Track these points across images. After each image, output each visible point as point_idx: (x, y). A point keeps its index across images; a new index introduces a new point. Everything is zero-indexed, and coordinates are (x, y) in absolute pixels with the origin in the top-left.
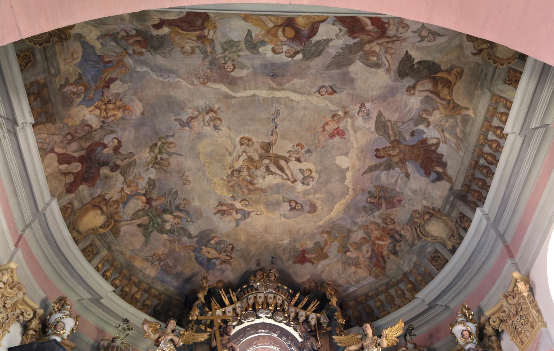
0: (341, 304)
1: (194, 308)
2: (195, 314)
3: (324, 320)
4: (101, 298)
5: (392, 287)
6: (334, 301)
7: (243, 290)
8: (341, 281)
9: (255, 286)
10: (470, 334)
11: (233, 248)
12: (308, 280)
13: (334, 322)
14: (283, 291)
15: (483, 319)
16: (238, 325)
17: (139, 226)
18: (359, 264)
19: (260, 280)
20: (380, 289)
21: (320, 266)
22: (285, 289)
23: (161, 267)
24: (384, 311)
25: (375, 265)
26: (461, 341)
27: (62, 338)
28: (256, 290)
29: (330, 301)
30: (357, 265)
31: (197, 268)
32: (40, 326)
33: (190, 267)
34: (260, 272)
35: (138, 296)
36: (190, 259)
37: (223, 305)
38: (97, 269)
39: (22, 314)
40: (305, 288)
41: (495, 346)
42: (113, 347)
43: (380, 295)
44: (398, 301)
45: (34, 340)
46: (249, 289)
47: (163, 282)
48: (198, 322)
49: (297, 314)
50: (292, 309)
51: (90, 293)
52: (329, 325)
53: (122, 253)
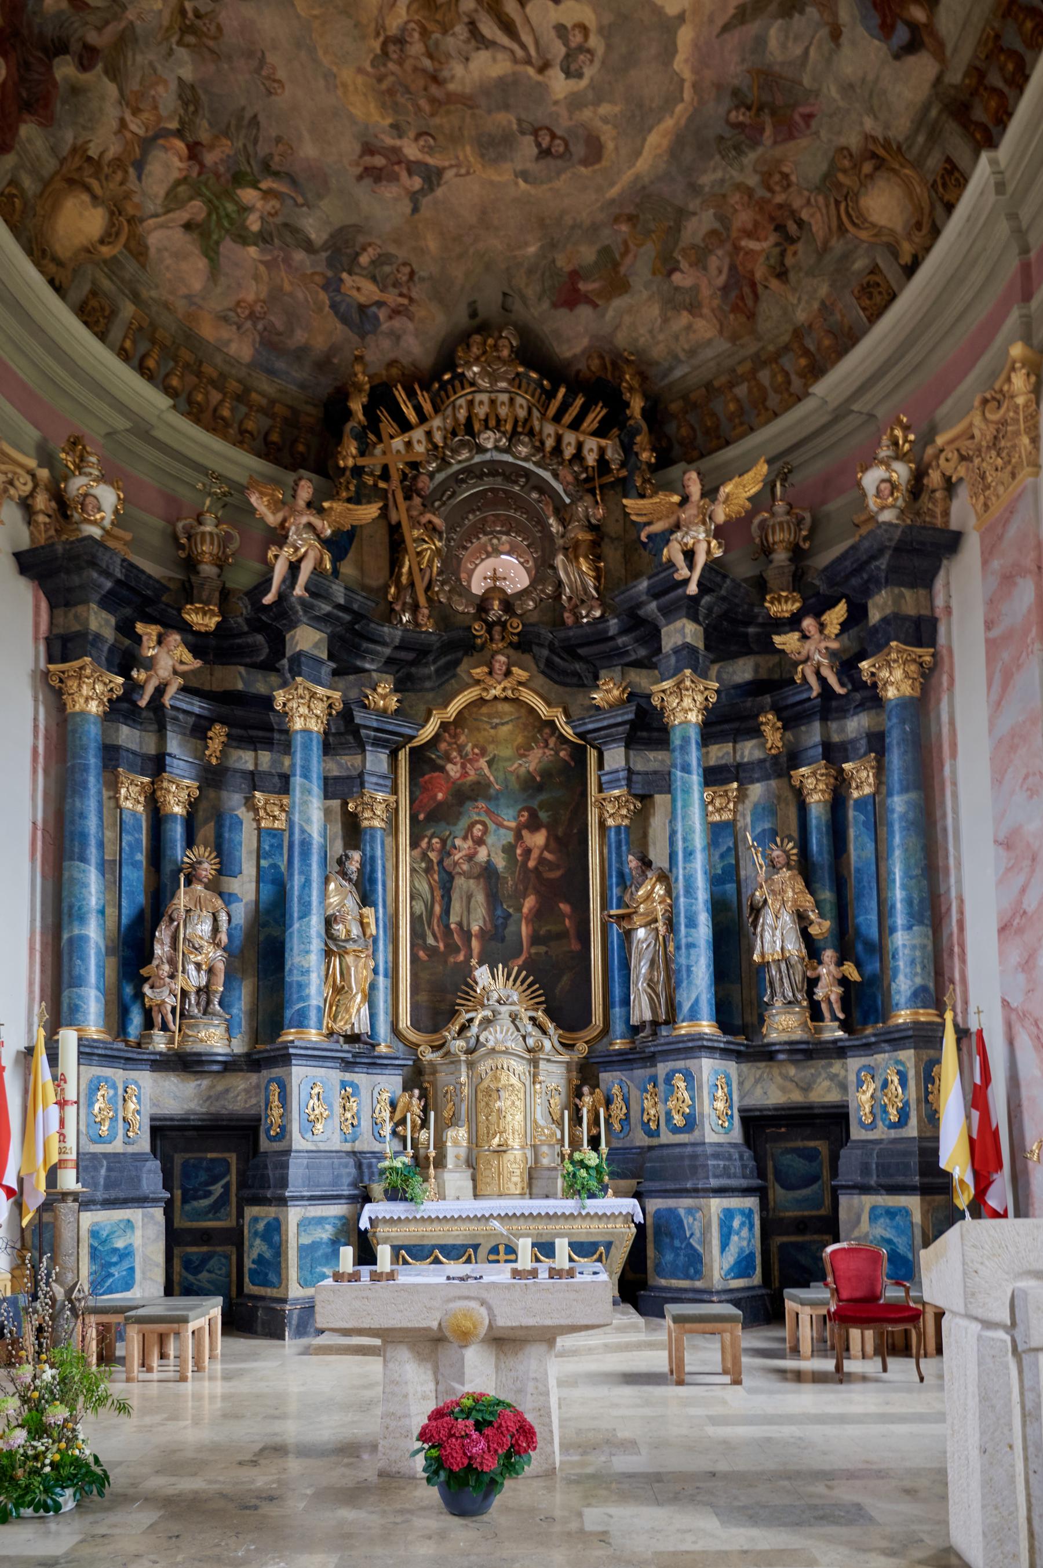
0: (654, 414)
1: (345, 439)
2: (349, 454)
3: (613, 454)
5: (764, 364)
6: (637, 404)
7: (443, 386)
8: (657, 352)
9: (469, 374)
11: (412, 274)
12: (583, 352)
13: (633, 459)
16: (439, 470)
17: (188, 226)
18: (700, 306)
19: (477, 360)
20: (740, 370)
21: (610, 313)
23: (260, 334)
24: (742, 424)
25: (735, 309)
27: (103, 529)
28: (472, 384)
29: (627, 405)
30: (693, 308)
31: (339, 330)
33: (322, 332)
34: (477, 338)
36: (320, 310)
37: (405, 426)
38: (124, 355)
40: (578, 372)
46: (457, 383)
47: (271, 372)
48: (358, 471)
50: (549, 429)
52: (623, 465)
53: (166, 306)
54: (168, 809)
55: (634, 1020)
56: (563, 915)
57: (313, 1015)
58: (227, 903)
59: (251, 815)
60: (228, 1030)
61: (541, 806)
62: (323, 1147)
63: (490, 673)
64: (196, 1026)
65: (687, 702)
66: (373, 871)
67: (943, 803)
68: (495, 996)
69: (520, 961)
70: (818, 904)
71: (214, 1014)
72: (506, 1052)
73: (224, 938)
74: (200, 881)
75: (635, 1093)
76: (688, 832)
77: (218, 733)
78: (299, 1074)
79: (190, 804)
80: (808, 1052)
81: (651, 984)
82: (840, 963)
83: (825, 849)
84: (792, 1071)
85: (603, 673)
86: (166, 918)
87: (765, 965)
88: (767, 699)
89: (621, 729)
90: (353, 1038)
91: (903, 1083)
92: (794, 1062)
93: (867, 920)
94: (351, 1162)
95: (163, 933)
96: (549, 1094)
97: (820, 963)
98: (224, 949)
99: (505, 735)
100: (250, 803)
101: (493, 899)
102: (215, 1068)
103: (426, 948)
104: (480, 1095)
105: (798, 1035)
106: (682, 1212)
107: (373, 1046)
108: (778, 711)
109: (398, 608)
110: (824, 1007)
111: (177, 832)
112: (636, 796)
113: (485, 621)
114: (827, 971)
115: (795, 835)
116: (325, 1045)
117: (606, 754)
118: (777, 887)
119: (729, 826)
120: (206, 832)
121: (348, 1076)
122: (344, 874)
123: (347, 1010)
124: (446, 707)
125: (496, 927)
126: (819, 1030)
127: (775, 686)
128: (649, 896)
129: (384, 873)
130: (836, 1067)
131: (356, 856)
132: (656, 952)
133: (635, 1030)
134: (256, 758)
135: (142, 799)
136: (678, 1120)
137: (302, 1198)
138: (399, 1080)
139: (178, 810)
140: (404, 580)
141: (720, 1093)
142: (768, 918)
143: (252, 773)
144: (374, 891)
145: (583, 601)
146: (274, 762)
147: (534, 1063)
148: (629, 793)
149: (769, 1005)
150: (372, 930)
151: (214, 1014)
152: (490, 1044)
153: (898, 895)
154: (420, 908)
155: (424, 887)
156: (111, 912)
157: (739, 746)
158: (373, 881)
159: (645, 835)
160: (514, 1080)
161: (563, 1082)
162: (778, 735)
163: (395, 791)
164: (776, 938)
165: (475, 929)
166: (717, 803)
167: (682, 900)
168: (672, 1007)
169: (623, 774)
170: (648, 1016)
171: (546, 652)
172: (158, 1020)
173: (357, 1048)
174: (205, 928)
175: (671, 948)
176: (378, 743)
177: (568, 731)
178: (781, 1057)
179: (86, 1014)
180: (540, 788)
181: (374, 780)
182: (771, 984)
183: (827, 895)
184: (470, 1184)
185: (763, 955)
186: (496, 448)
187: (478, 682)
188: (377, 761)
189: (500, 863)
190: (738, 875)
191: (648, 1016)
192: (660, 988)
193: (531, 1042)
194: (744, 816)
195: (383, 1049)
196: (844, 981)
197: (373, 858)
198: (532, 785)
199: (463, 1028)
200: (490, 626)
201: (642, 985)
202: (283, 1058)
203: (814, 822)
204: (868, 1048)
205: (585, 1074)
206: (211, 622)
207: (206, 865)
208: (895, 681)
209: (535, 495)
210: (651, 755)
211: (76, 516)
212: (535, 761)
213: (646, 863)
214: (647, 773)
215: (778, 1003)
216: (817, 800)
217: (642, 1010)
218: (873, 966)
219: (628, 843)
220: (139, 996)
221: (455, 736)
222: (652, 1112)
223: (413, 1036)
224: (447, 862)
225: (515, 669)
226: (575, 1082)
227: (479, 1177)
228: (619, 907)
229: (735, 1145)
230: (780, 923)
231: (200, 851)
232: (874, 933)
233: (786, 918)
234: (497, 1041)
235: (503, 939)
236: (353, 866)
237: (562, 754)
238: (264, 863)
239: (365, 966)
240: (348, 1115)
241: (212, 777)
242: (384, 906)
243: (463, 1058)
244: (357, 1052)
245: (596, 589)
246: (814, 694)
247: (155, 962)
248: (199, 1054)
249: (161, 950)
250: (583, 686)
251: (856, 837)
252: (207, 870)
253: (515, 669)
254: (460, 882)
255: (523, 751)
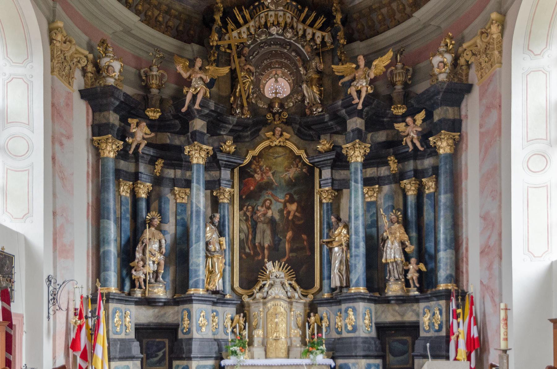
4: (132, 30)
10: (445, 65)
14: (292, 7)
15: (460, 49)
22: (294, 6)
26: (436, 71)
27: (115, 79)
32: (94, 69)
35: (161, 19)
39: (79, 62)
41: (464, 74)
42: (153, 75)
43: (383, 8)
44: (398, 16)
45: (93, 80)
49: (305, 31)
51: (120, 25)
54: (139, 195)
55: (333, 286)
56: (303, 240)
57: (201, 283)
58: (164, 235)
59: (173, 197)
60: (165, 289)
61: (295, 193)
62: (205, 337)
63: (274, 135)
64: (153, 287)
65: (357, 153)
66: (224, 221)
67: (461, 198)
68: (275, 275)
69: (285, 259)
70: (410, 238)
71: (160, 282)
72: (280, 299)
73: (164, 250)
74: (154, 226)
75: (332, 316)
76: (357, 208)
77: (160, 163)
78: (196, 307)
79: (148, 193)
80: (403, 300)
81: (340, 271)
82: (417, 264)
83: (414, 214)
84: (397, 308)
85: (322, 136)
86: (141, 242)
87: (387, 264)
88: (391, 150)
89: (329, 161)
90: (216, 292)
91: (441, 314)
92: (398, 304)
93: (430, 246)
94: (216, 343)
95: (139, 248)
96: (296, 317)
97: (410, 263)
98: (164, 255)
99: (281, 161)
100: (172, 191)
101: (274, 232)
102: (161, 304)
103: (246, 254)
104: (268, 316)
105: (400, 293)
106: (350, 365)
107: (224, 295)
108: (396, 156)
109: (235, 107)
110: (411, 281)
111: (143, 205)
112: (335, 190)
113: (271, 112)
114: (412, 267)
115: (401, 208)
116: (206, 296)
117: (323, 171)
118: (393, 231)
119: (374, 203)
120: (155, 205)
121: (214, 308)
122: (213, 223)
123: (214, 281)
124: (255, 149)
125: (275, 245)
126: (408, 291)
127: (394, 144)
128: (340, 234)
129: (228, 222)
130: (415, 306)
131: (218, 215)
132: (342, 257)
133: (333, 290)
134: (175, 172)
135: (129, 191)
136: (350, 328)
137: (197, 357)
138: (235, 309)
139: (144, 196)
140: (237, 94)
141: (367, 317)
142: (389, 244)
143: (173, 179)
144: (224, 230)
145: (314, 105)
146: (182, 174)
147: (291, 303)
148: (333, 189)
149: (389, 280)
150: (224, 247)
151: (160, 282)
152: (273, 295)
153: (441, 236)
154: (243, 236)
155: (245, 227)
156: (119, 239)
157: (379, 169)
158: (224, 226)
159: (339, 207)
160: (282, 310)
161: (303, 311)
162: (396, 165)
163: (233, 187)
164: (392, 253)
165: (266, 245)
166: (370, 193)
167: (353, 237)
168: (348, 281)
169: (330, 181)
170: (338, 284)
171: (298, 126)
172: (137, 284)
173: (218, 296)
174: (156, 246)
175: (348, 256)
176: (226, 166)
177: (307, 161)
178: (393, 302)
179: (110, 282)
180: (294, 185)
181: (225, 182)
182: (390, 271)
183: (414, 234)
184: (264, 353)
185: (386, 260)
186: (277, 34)
187: (268, 138)
188: (226, 174)
189: (277, 217)
190: (377, 224)
191: (338, 284)
192: (344, 272)
193: (289, 294)
194: (381, 199)
195: (228, 297)
196: (419, 271)
197: (224, 216)
198: (291, 184)
199: (261, 288)
200: (274, 114)
201: (336, 271)
202: (189, 300)
203: (409, 203)
204: (428, 299)
205: (312, 308)
206: (158, 115)
207: (156, 220)
208: (444, 146)
209: (293, 54)
210: (342, 172)
211: (104, 74)
212: (292, 173)
213: (339, 220)
214: (340, 180)
215: (392, 279)
216: (411, 193)
217: (336, 282)
218: (432, 265)
219: (331, 210)
220: (130, 274)
221: (258, 162)
222: (339, 324)
223: (240, 291)
224: (254, 217)
225: (284, 133)
226: (308, 311)
227: (268, 350)
228: (327, 238)
229: (373, 338)
230: (393, 247)
231: (154, 213)
232: (432, 251)
233: (396, 244)
234: (276, 294)
235: (278, 250)
236: (216, 220)
237: (304, 170)
238: (178, 218)
239: (221, 262)
240: (214, 324)
241: (158, 181)
242: (229, 236)
243: (262, 300)
244: (217, 298)
245: (320, 99)
246: (410, 150)
247: (136, 261)
248: (155, 299)
249: (138, 255)
250: (313, 140)
251: (427, 210)
252: (156, 222)
253: (284, 133)
254: (260, 226)
255: (288, 169)
